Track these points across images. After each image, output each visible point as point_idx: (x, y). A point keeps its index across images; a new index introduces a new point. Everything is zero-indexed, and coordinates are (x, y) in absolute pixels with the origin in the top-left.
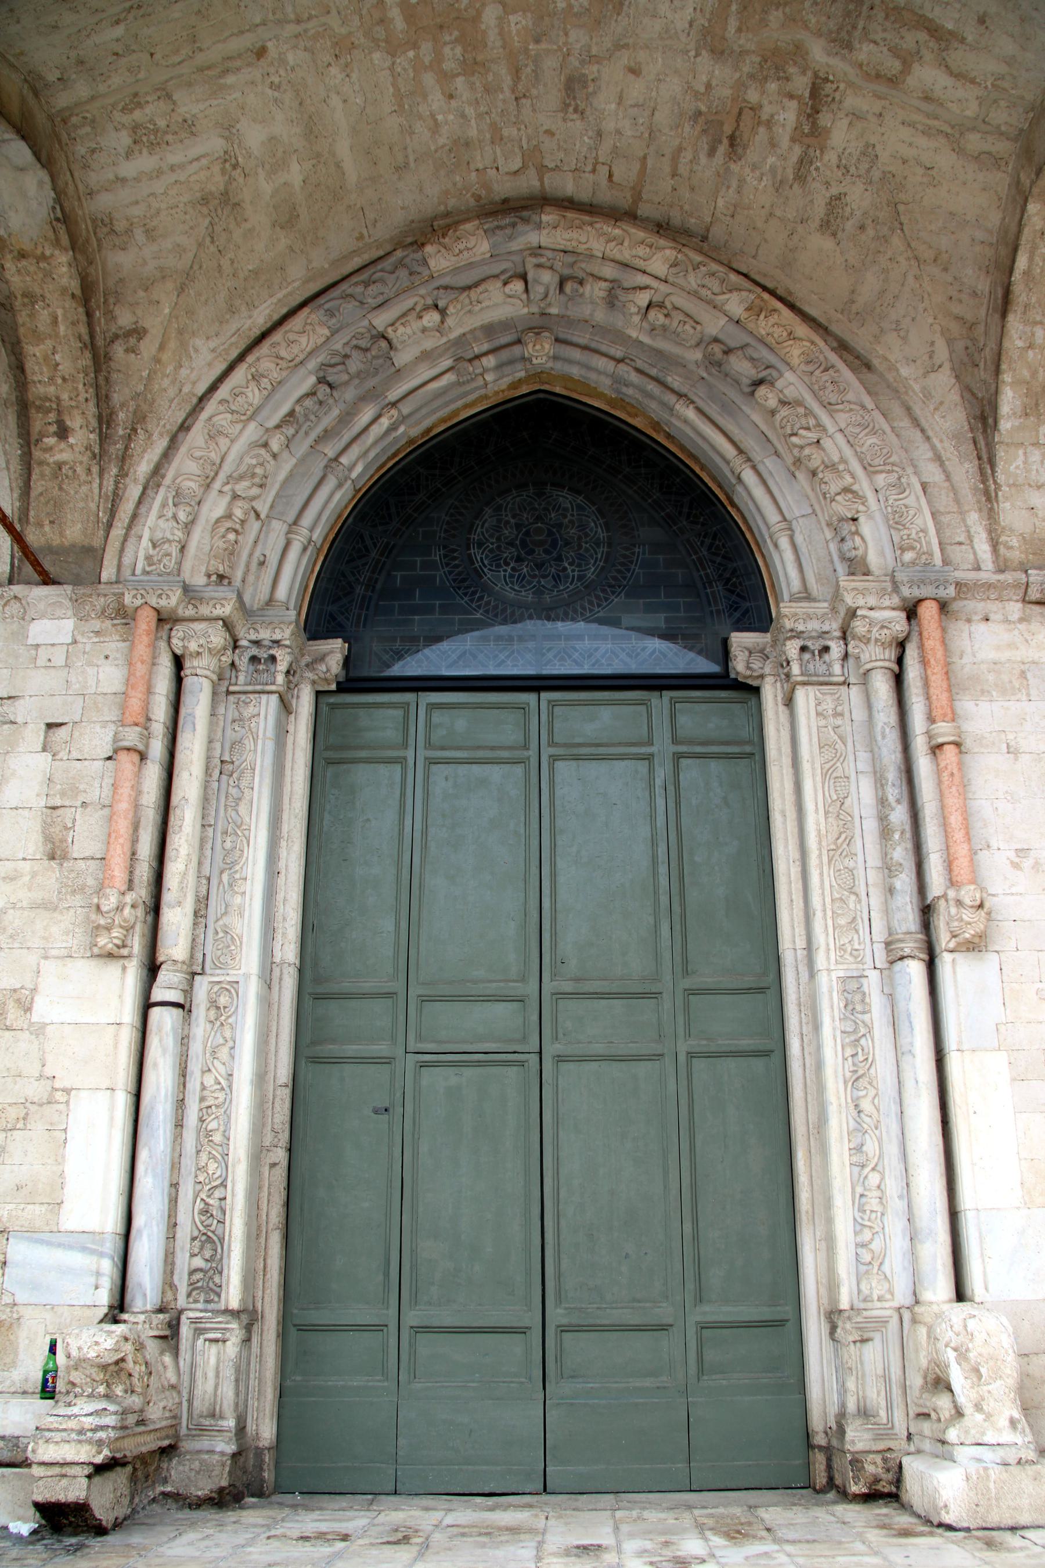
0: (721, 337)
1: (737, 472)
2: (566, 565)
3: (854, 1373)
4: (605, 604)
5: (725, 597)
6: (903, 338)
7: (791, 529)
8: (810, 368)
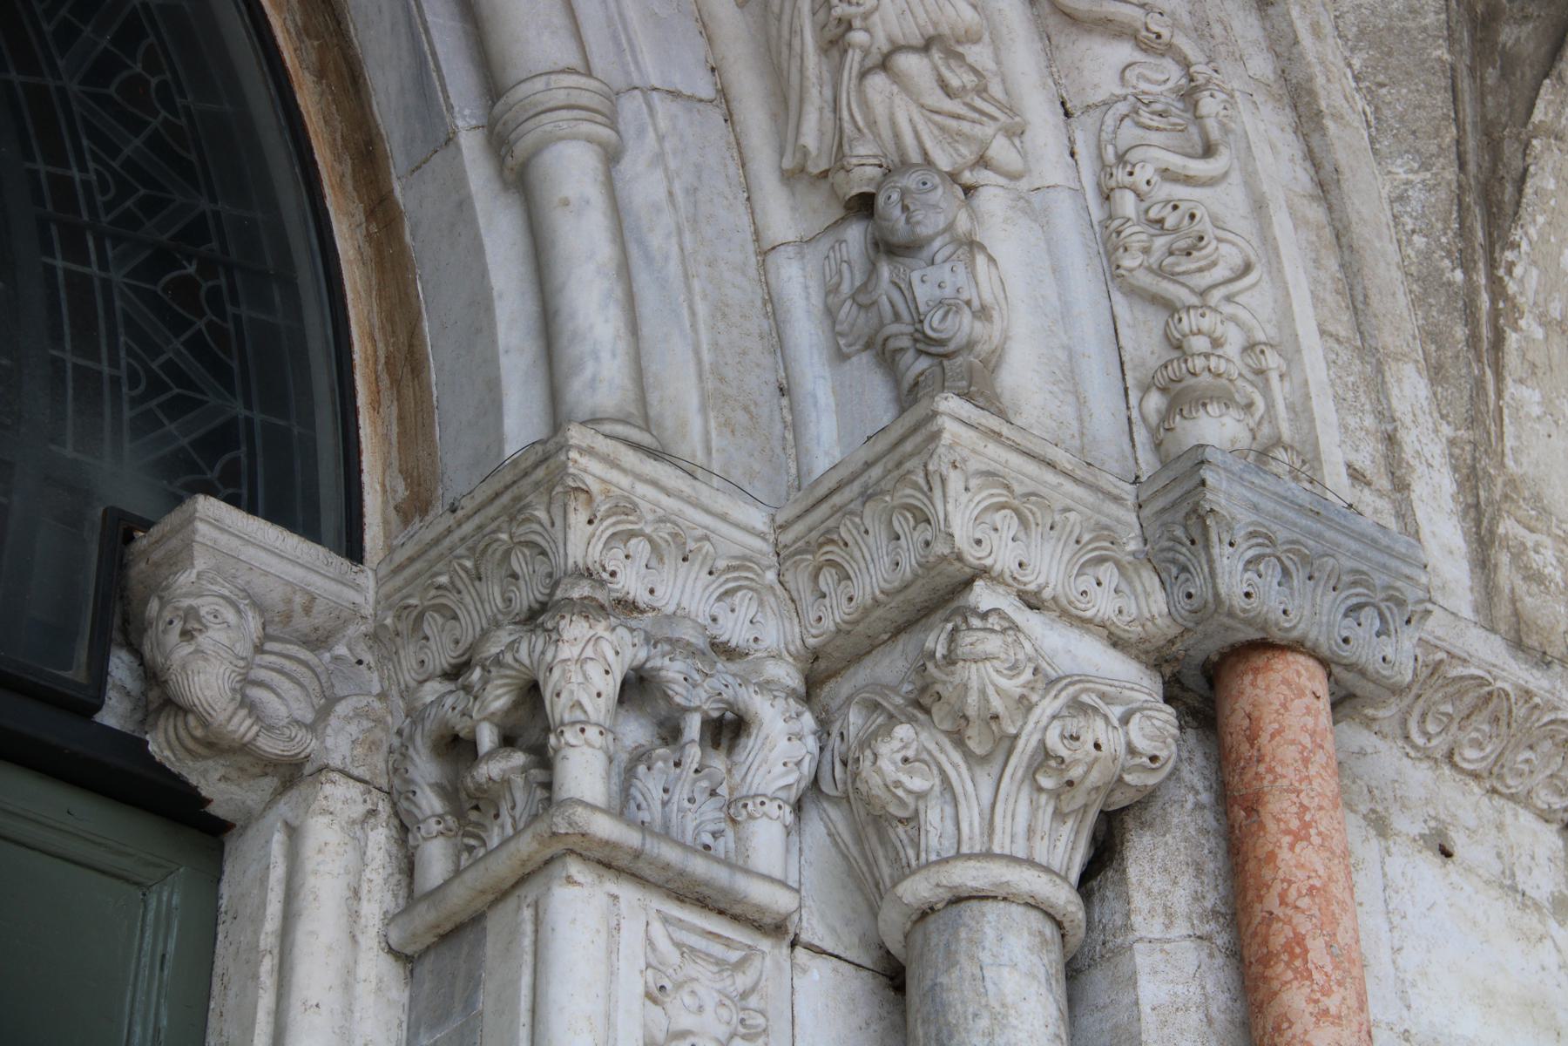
7: (612, 122)
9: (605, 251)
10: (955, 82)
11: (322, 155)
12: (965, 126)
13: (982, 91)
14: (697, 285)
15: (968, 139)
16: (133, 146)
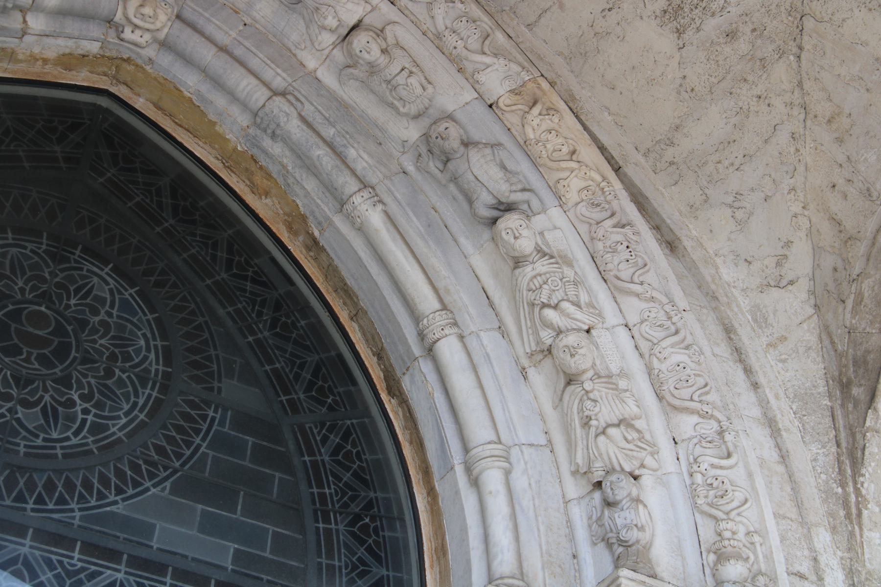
0: (459, 115)
1: (431, 337)
2: (76, 397)
4: (131, 492)
5: (346, 546)
6: (739, 223)
7: (507, 459)
8: (597, 215)
9: (505, 510)
10: (630, 438)
11: (412, 472)
12: (635, 454)
13: (642, 439)
14: (540, 519)
15: (636, 458)
16: (347, 477)
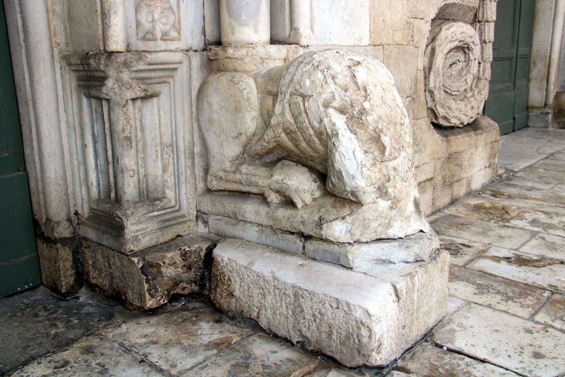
3: (134, 144)
